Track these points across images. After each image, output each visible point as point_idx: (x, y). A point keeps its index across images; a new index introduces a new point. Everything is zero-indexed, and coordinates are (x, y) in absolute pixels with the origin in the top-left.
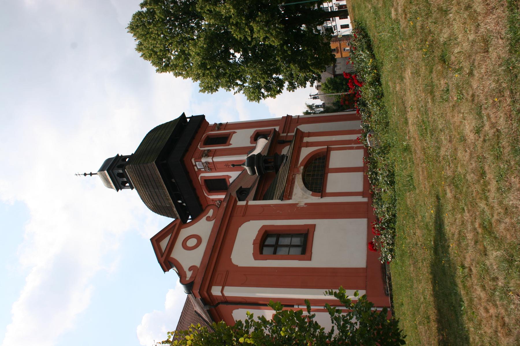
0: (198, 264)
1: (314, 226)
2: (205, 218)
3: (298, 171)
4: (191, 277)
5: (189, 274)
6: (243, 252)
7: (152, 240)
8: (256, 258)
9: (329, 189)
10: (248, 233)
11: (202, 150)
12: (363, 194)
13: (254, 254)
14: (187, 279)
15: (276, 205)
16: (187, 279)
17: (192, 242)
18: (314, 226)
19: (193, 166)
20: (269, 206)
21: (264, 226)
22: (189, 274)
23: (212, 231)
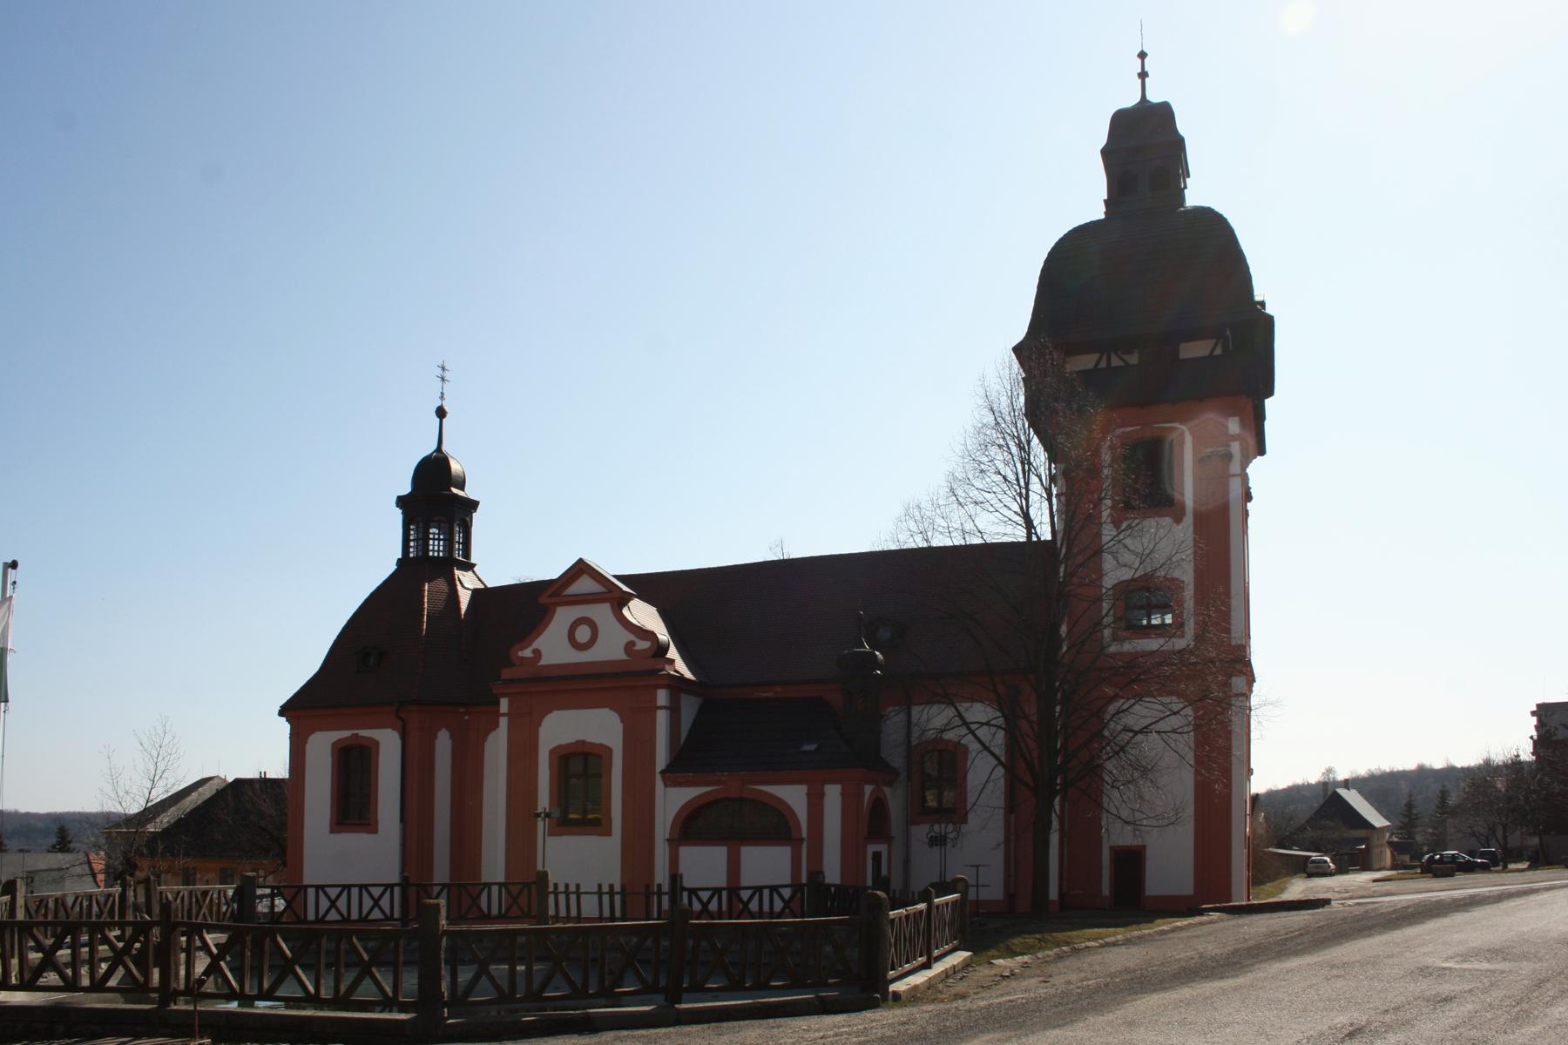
0: (546, 660)
1: (608, 833)
2: (632, 637)
5: (527, 653)
6: (562, 727)
7: (581, 561)
8: (552, 752)
9: (686, 853)
10: (599, 726)
18: (608, 833)
21: (609, 750)
22: (527, 653)
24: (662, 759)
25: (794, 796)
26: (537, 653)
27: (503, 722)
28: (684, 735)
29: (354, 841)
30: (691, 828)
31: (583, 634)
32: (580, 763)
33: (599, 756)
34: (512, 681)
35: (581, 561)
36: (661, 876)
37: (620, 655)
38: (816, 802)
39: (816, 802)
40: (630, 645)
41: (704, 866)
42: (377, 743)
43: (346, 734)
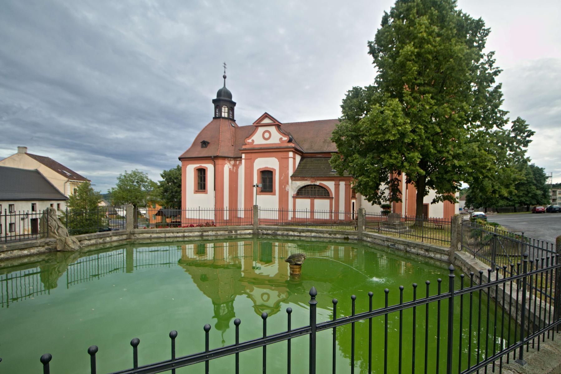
1: (275, 195)
2: (281, 136)
3: (312, 182)
5: (250, 141)
6: (261, 163)
7: (266, 113)
8: (258, 170)
9: (298, 200)
12: (294, 217)
15: (288, 174)
18: (275, 195)
21: (275, 170)
22: (250, 141)
23: (273, 144)
24: (291, 172)
25: (330, 185)
26: (253, 141)
27: (243, 161)
28: (297, 166)
30: (301, 193)
31: (267, 135)
32: (267, 174)
34: (245, 150)
35: (266, 113)
36: (291, 207)
37: (278, 141)
38: (337, 187)
39: (337, 187)
40: (281, 139)
41: (304, 204)
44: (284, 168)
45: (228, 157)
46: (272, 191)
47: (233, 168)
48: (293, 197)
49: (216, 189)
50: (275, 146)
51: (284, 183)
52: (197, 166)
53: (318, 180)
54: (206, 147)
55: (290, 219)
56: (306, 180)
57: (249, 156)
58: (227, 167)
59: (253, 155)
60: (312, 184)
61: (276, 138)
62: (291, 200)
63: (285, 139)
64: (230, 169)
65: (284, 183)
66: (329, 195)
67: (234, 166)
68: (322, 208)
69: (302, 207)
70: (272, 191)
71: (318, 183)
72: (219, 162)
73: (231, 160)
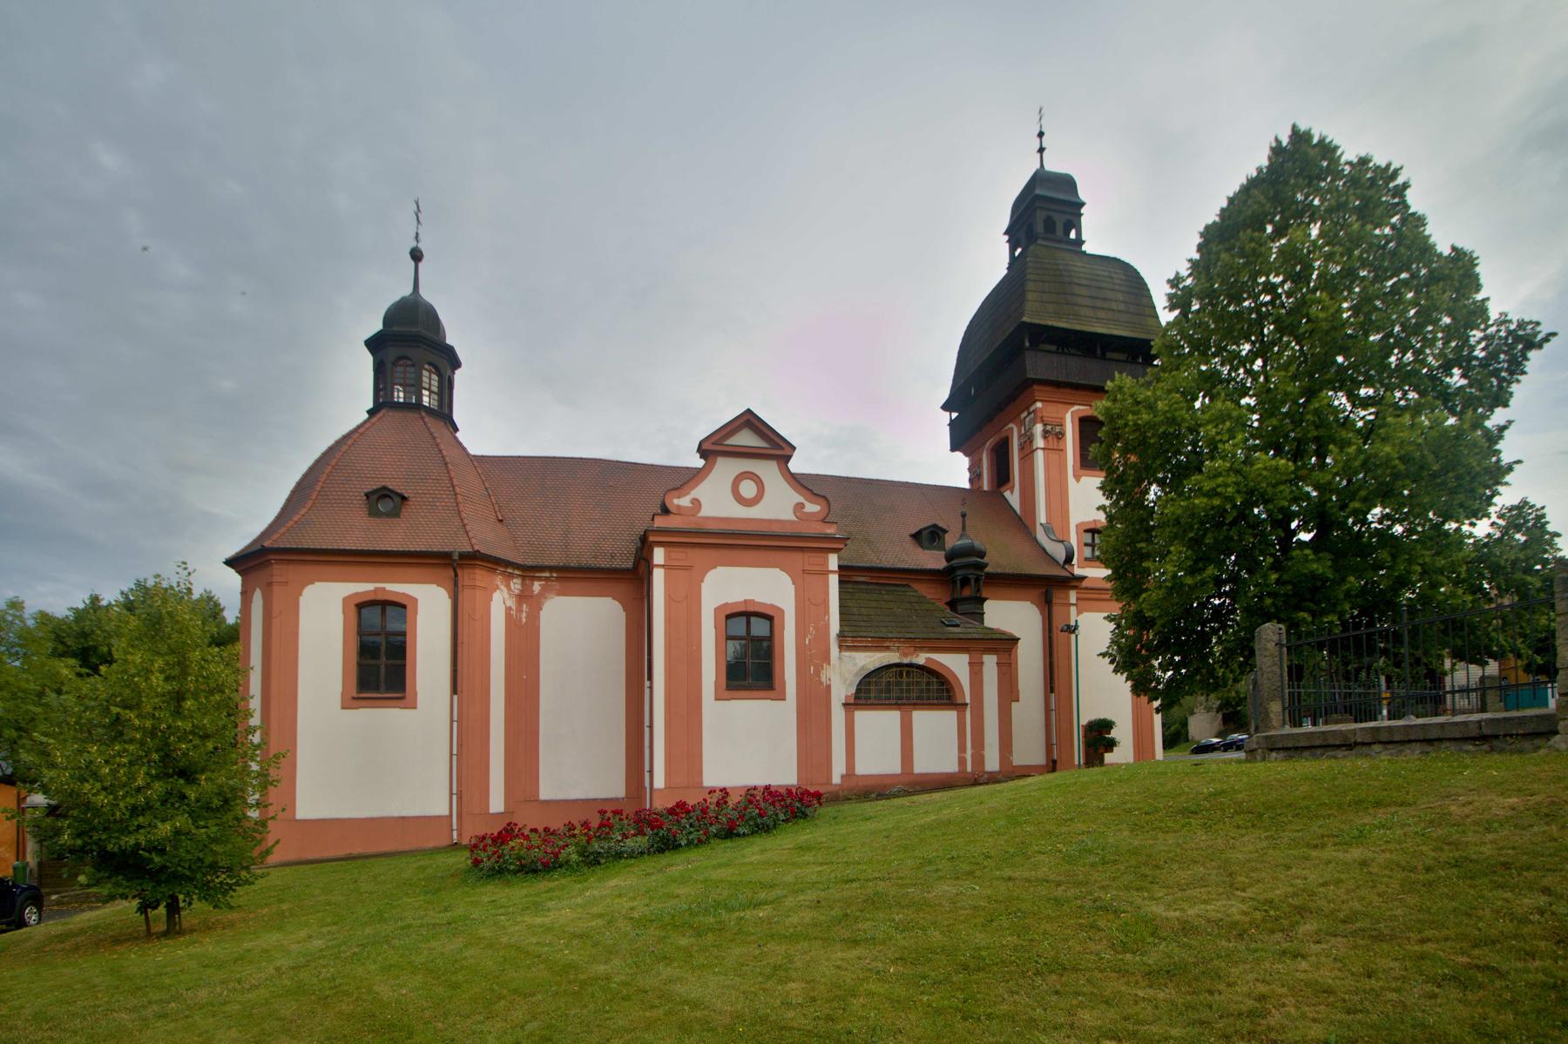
0: (705, 512)
2: (800, 499)
3: (906, 655)
4: (679, 507)
8: (717, 610)
9: (862, 717)
10: (767, 585)
11: (1063, 419)
12: (850, 774)
13: (726, 605)
14: (676, 501)
15: (827, 626)
16: (676, 501)
17: (748, 489)
19: (1028, 408)
20: (827, 612)
21: (782, 611)
22: (685, 502)
23: (770, 521)
25: (956, 664)
26: (697, 503)
29: (384, 718)
30: (873, 691)
33: (770, 618)
37: (789, 515)
38: (976, 669)
40: (800, 506)
42: (415, 601)
43: (370, 587)
44: (809, 607)
45: (508, 564)
46: (771, 687)
47: (519, 610)
48: (845, 705)
49: (463, 684)
50: (777, 530)
51: (813, 658)
52: (364, 588)
53: (922, 649)
54: (394, 513)
55: (836, 779)
56: (888, 648)
57: (680, 555)
58: (500, 600)
59: (697, 556)
60: (906, 661)
61: (779, 504)
62: (838, 716)
63: (812, 508)
64: (508, 609)
65: (813, 658)
66: (949, 698)
67: (522, 597)
68: (936, 740)
69: (876, 743)
70: (771, 687)
71: (921, 659)
72: (480, 576)
73: (511, 576)
